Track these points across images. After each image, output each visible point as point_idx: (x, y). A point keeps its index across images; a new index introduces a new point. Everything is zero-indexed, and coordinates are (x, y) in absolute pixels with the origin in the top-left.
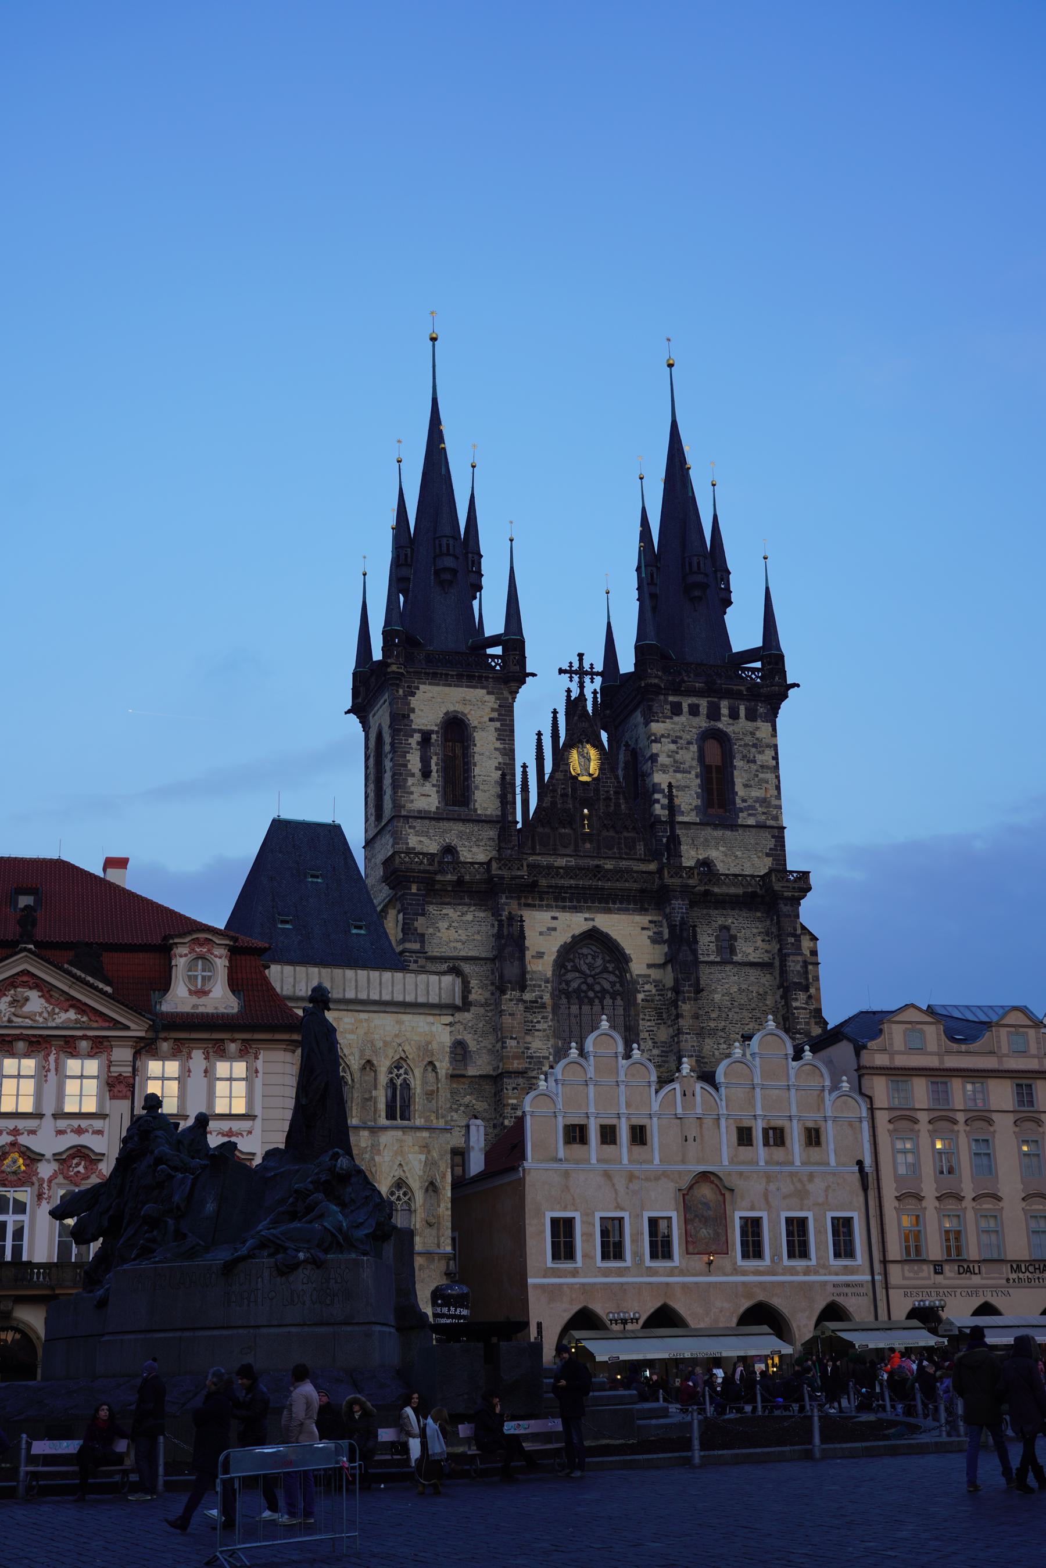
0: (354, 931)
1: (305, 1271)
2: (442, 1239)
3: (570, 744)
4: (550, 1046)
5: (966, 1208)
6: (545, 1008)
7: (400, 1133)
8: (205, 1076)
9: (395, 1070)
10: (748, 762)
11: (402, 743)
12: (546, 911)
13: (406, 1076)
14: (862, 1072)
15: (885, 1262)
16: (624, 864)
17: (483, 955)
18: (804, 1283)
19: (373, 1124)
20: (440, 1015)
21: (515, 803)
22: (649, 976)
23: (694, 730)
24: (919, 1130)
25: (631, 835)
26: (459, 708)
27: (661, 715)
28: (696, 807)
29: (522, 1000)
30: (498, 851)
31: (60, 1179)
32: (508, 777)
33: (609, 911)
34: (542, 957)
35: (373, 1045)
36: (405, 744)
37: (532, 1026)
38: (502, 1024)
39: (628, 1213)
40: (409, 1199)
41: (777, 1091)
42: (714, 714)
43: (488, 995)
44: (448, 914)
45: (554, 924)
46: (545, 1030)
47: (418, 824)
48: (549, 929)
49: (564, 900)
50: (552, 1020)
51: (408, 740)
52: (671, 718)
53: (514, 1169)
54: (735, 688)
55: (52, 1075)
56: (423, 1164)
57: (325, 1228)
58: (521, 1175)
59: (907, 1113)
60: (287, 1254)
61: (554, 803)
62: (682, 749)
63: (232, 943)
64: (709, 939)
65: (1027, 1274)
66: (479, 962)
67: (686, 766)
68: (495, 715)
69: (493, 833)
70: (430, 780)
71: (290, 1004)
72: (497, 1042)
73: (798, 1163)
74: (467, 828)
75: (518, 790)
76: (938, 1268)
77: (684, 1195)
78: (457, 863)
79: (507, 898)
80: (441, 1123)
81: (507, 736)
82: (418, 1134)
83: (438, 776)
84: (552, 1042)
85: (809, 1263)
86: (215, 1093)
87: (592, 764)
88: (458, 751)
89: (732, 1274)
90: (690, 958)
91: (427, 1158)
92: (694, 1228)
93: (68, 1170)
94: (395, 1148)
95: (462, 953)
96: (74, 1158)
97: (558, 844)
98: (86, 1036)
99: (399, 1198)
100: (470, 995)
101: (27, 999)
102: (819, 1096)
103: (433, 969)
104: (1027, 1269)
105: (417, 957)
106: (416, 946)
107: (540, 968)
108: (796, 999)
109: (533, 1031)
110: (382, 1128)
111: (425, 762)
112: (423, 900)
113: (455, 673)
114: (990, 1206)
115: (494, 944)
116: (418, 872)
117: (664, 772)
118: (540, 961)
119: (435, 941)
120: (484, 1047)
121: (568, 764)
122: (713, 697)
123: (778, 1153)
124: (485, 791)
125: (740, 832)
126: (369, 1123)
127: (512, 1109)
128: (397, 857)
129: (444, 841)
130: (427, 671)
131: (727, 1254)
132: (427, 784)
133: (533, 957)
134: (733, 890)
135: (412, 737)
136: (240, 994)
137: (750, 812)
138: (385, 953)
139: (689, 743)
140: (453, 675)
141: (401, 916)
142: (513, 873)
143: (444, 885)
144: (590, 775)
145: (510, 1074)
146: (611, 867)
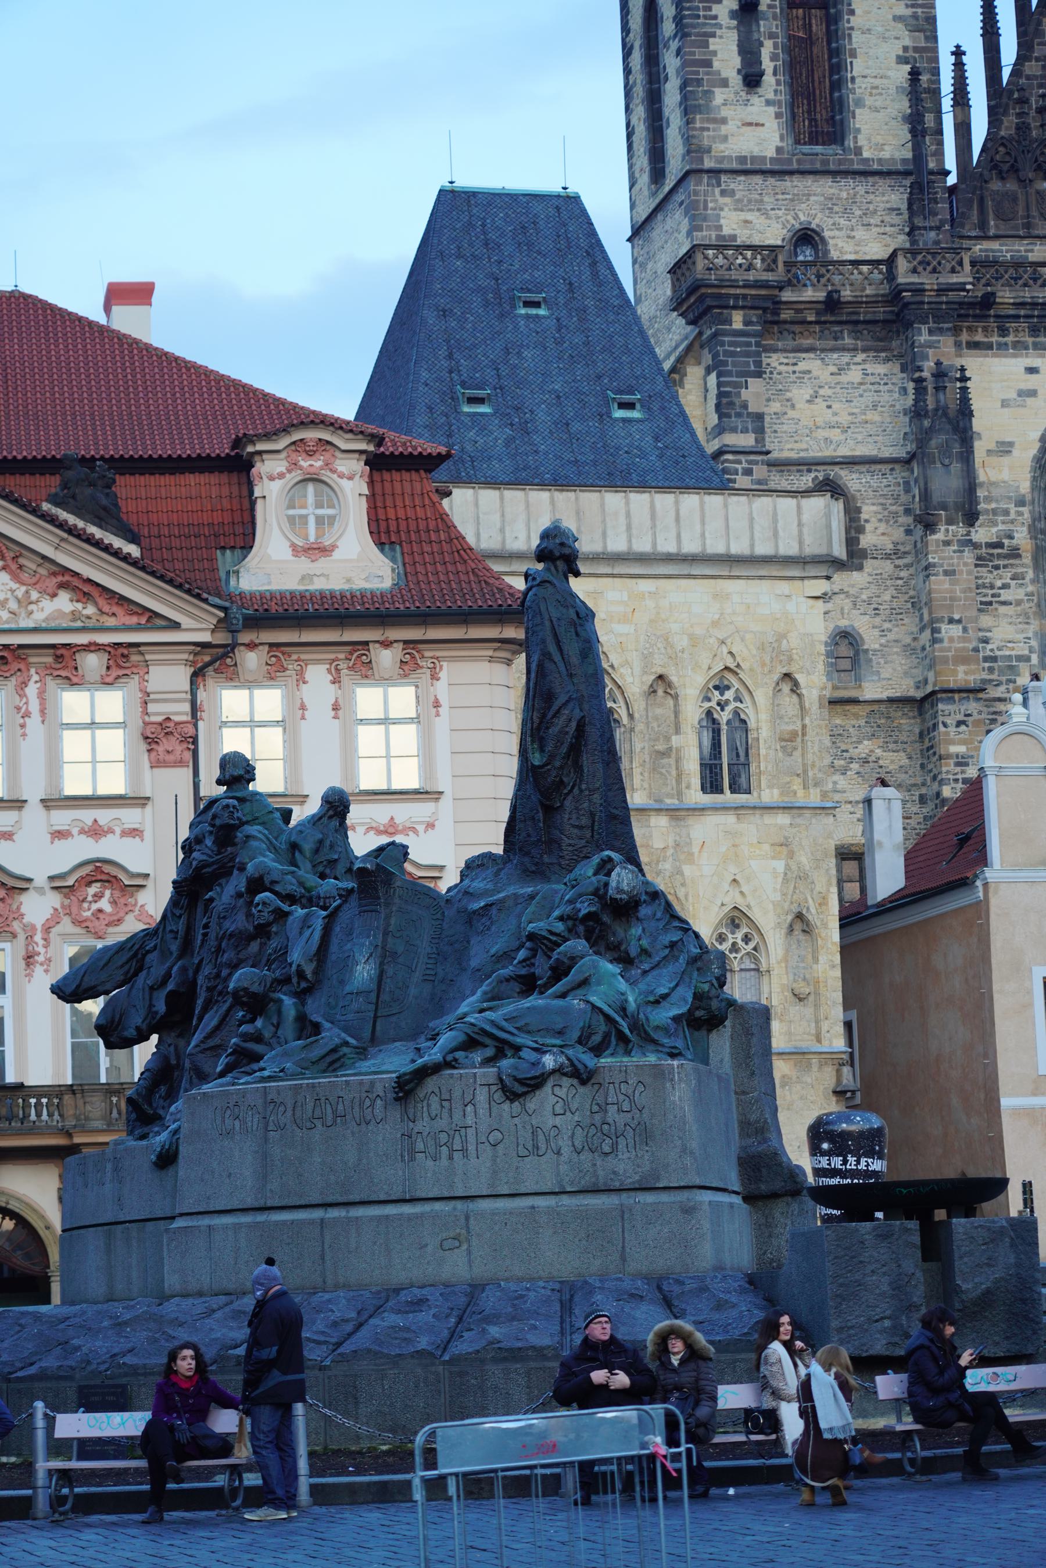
1: (557, 1090)
2: (825, 1026)
4: (1030, 635)
6: (1019, 556)
7: (730, 819)
8: (336, 717)
9: (716, 693)
11: (698, 17)
12: (1015, 356)
13: (738, 704)
17: (887, 453)
19: (676, 802)
20: (802, 578)
21: (940, 132)
29: (970, 542)
30: (909, 234)
31: (66, 925)
32: (924, 78)
35: (668, 644)
36: (705, 17)
37: (993, 596)
38: (930, 593)
40: (755, 949)
43: (898, 534)
44: (809, 372)
45: (1032, 382)
46: (1019, 603)
47: (738, 185)
48: (1021, 393)
50: (1033, 581)
51: (710, 9)
53: (964, 883)
55: (34, 723)
56: (780, 880)
57: (594, 1007)
58: (981, 894)
60: (520, 1058)
61: (1022, 128)
63: (371, 448)
66: (879, 467)
69: (896, 197)
70: (760, 90)
71: (497, 567)
72: (922, 630)
75: (947, 103)
78: (824, 264)
79: (931, 332)
80: (814, 798)
82: (770, 819)
83: (778, 83)
86: (356, 750)
88: (818, 28)
91: (788, 867)
93: (80, 908)
94: (724, 849)
95: (844, 451)
96: (89, 884)
97: (1035, 214)
98: (95, 644)
99: (734, 948)
100: (861, 537)
103: (784, 485)
105: (750, 462)
106: (747, 440)
107: (1005, 475)
109: (995, 605)
110: (694, 809)
111: (749, 52)
112: (758, 344)
115: (908, 430)
116: (744, 287)
118: (1006, 460)
119: (785, 428)
120: (896, 641)
126: (668, 801)
127: (958, 764)
128: (699, 257)
129: (796, 217)
132: (755, 100)
133: (989, 452)
136: (393, 550)
138: (684, 456)
141: (712, 379)
142: (941, 280)
145: (949, 692)
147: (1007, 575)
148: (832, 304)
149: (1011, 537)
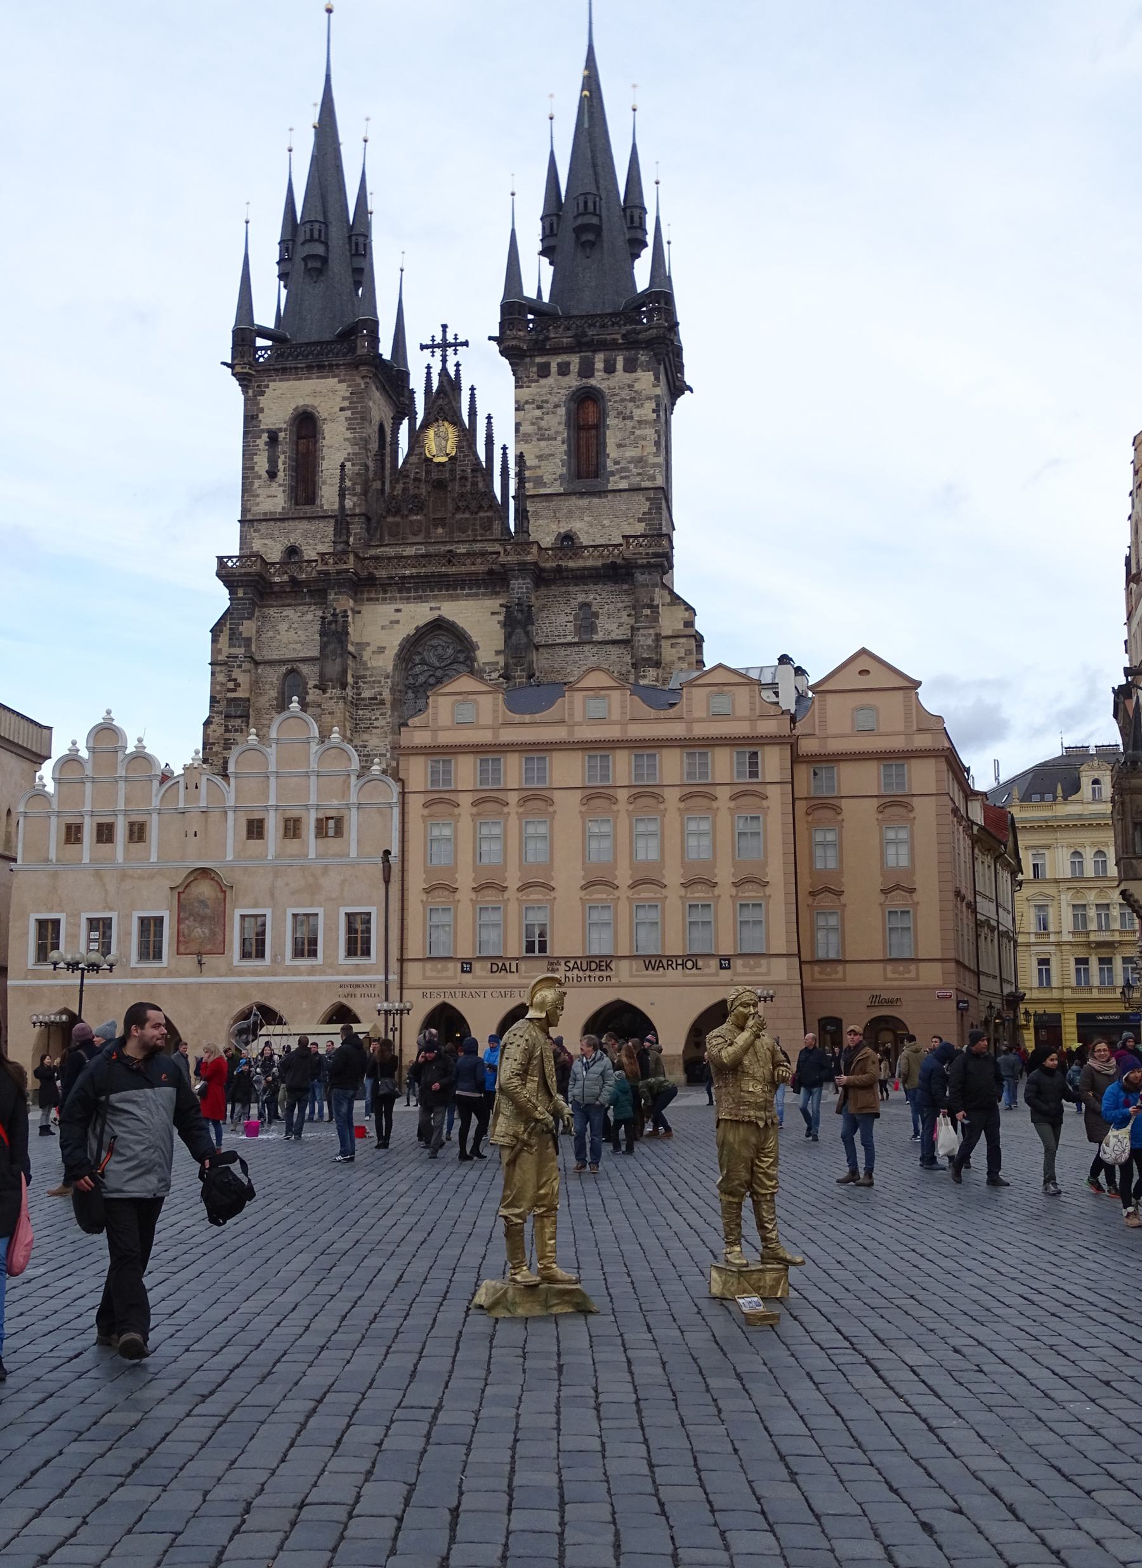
3: (426, 425)
5: (508, 899)
10: (624, 419)
12: (389, 604)
14: (399, 751)
15: (402, 961)
16: (477, 547)
18: (307, 983)
22: (497, 663)
23: (563, 391)
24: (459, 815)
25: (489, 514)
26: (308, 401)
27: (526, 379)
28: (561, 476)
33: (455, 598)
39: (116, 913)
41: (296, 778)
42: (587, 370)
46: (382, 727)
47: (263, 527)
48: (392, 622)
49: (409, 590)
52: (537, 381)
54: (608, 337)
59: (446, 796)
62: (548, 414)
64: (567, 619)
65: (576, 971)
67: (552, 432)
68: (346, 404)
70: (277, 480)
73: (312, 855)
74: (313, 526)
76: (467, 966)
77: (179, 893)
79: (336, 594)
81: (358, 424)
83: (285, 475)
84: (390, 738)
87: (449, 443)
89: (226, 975)
90: (524, 640)
92: (189, 928)
95: (302, 655)
102: (345, 781)
107: (380, 664)
108: (645, 677)
111: (273, 461)
113: (303, 365)
114: (540, 897)
117: (527, 442)
118: (382, 655)
121: (423, 446)
122: (586, 351)
123: (293, 845)
124: (332, 485)
125: (609, 498)
129: (289, 541)
130: (276, 367)
131: (223, 953)
132: (274, 485)
133: (373, 652)
134: (590, 563)
135: (260, 438)
137: (622, 474)
140: (302, 368)
143: (281, 587)
144: (447, 455)
146: (464, 551)
147: (378, 713)
148: (294, 581)
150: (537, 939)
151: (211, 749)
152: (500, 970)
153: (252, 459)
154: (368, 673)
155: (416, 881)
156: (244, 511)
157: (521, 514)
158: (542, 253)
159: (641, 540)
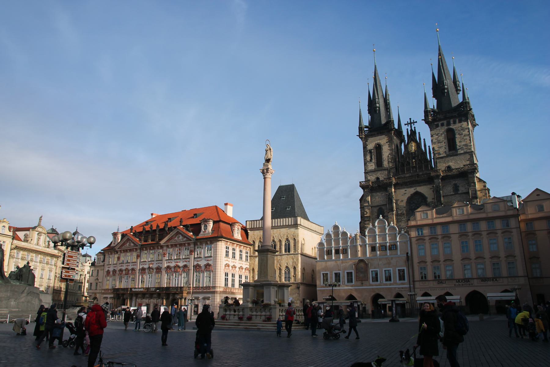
0: (287, 209)
7: (287, 256)
15: (414, 281)
22: (433, 202)
33: (420, 186)
34: (403, 201)
42: (448, 124)
45: (406, 192)
46: (404, 220)
48: (404, 194)
49: (408, 185)
52: (436, 129)
64: (451, 188)
82: (291, 255)
85: (391, 282)
89: (369, 286)
95: (382, 204)
101: (179, 237)
104: (462, 281)
107: (402, 204)
108: (474, 202)
114: (450, 263)
117: (435, 144)
118: (402, 202)
132: (372, 163)
133: (400, 202)
139: (442, 134)
146: (421, 174)
149: (403, 212)
150: (424, 276)
151: (362, 229)
152: (440, 283)
153: (366, 157)
154: (399, 207)
155: (416, 260)
156: (365, 170)
157: (436, 164)
158: (434, 97)
159: (468, 165)
